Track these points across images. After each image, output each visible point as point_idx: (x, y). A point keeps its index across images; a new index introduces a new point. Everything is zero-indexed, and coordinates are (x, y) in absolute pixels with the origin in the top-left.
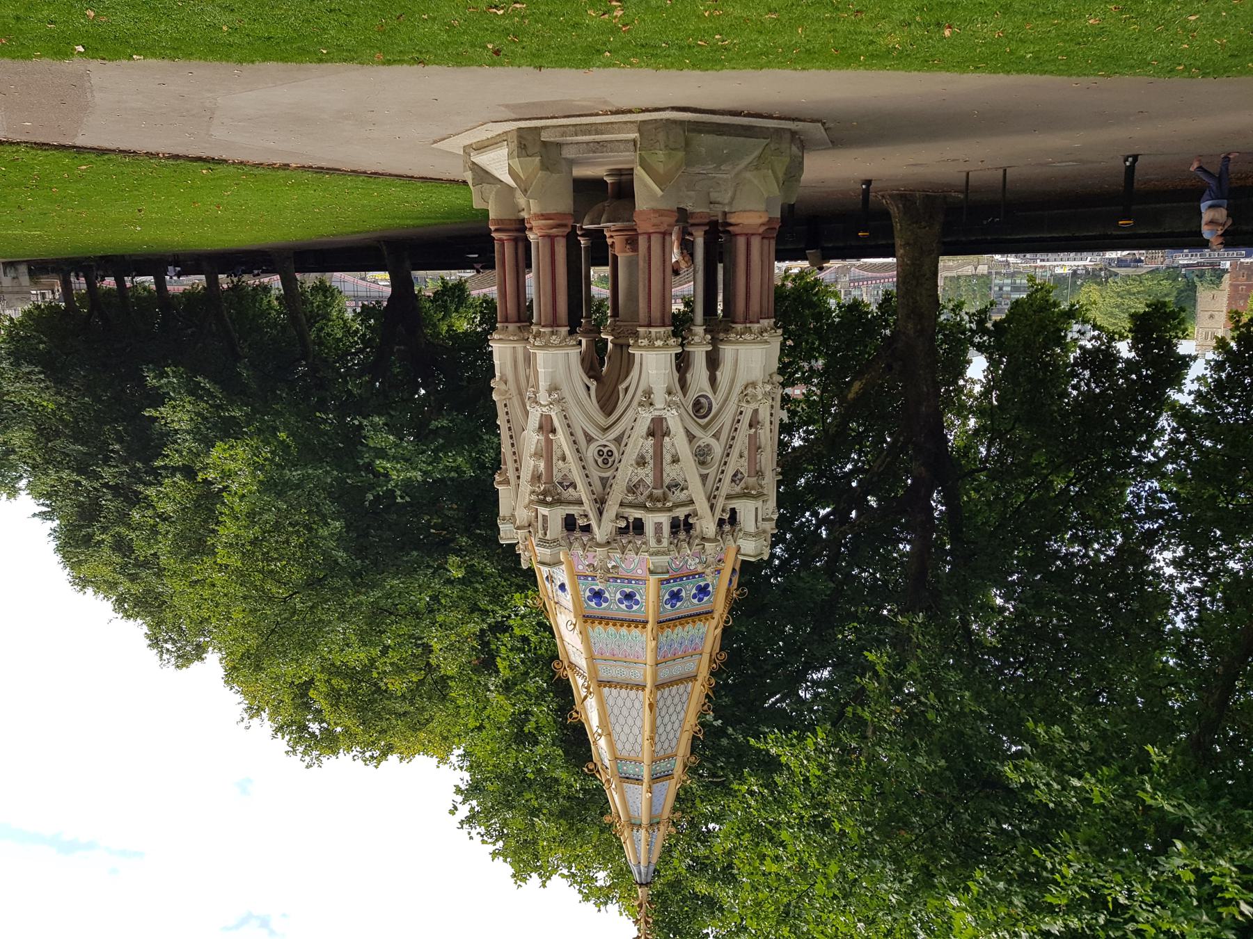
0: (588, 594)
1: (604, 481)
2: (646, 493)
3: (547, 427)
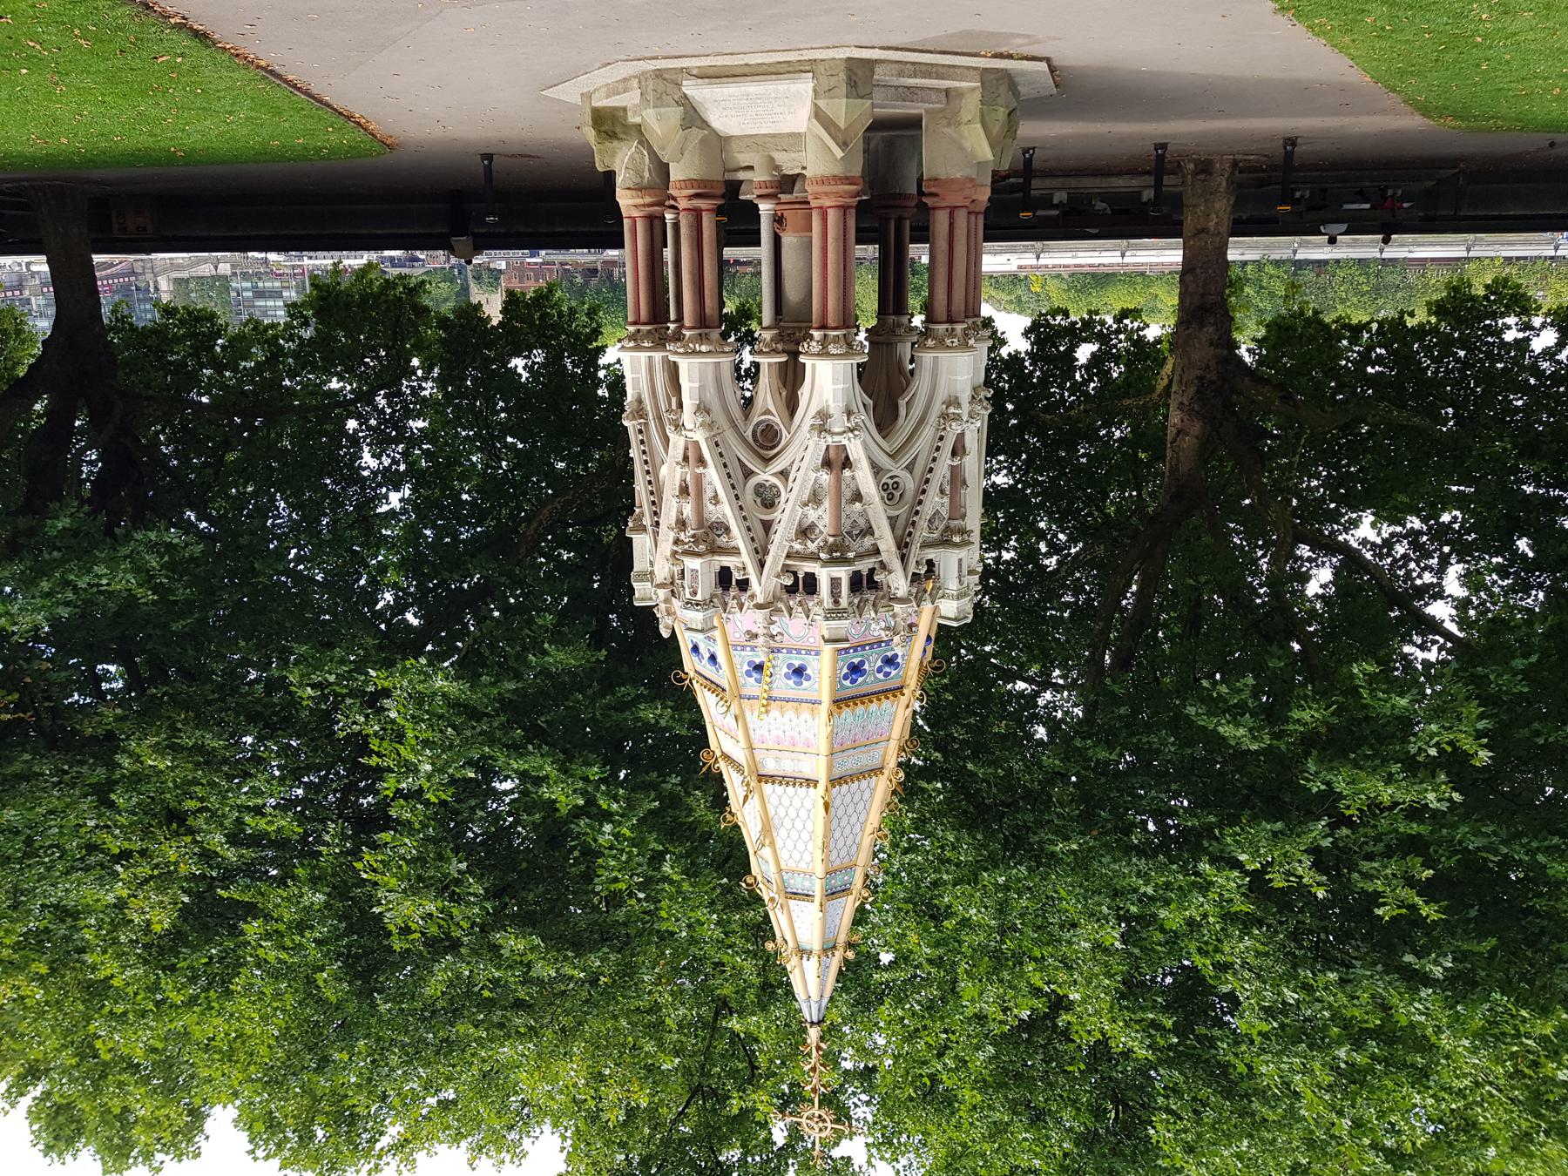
0: (845, 670)
1: (893, 521)
2: (942, 527)
3: (837, 462)
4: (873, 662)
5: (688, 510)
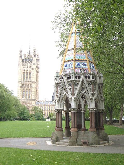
4: (68, 67)
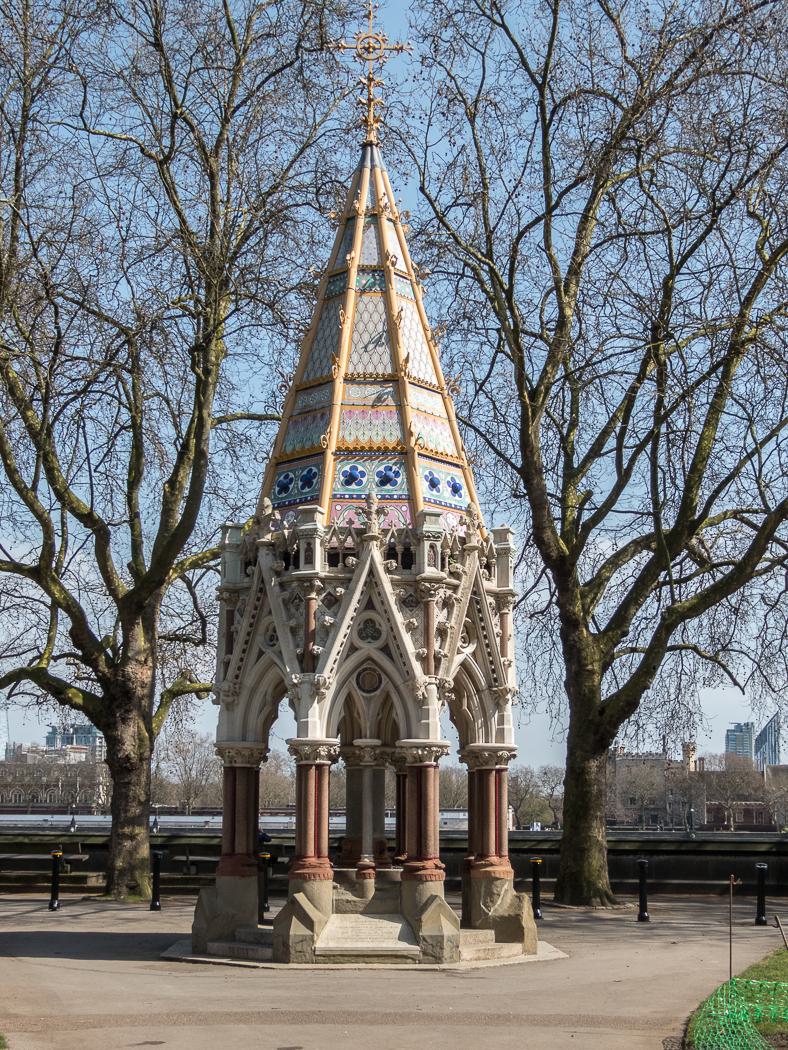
5: (438, 616)
